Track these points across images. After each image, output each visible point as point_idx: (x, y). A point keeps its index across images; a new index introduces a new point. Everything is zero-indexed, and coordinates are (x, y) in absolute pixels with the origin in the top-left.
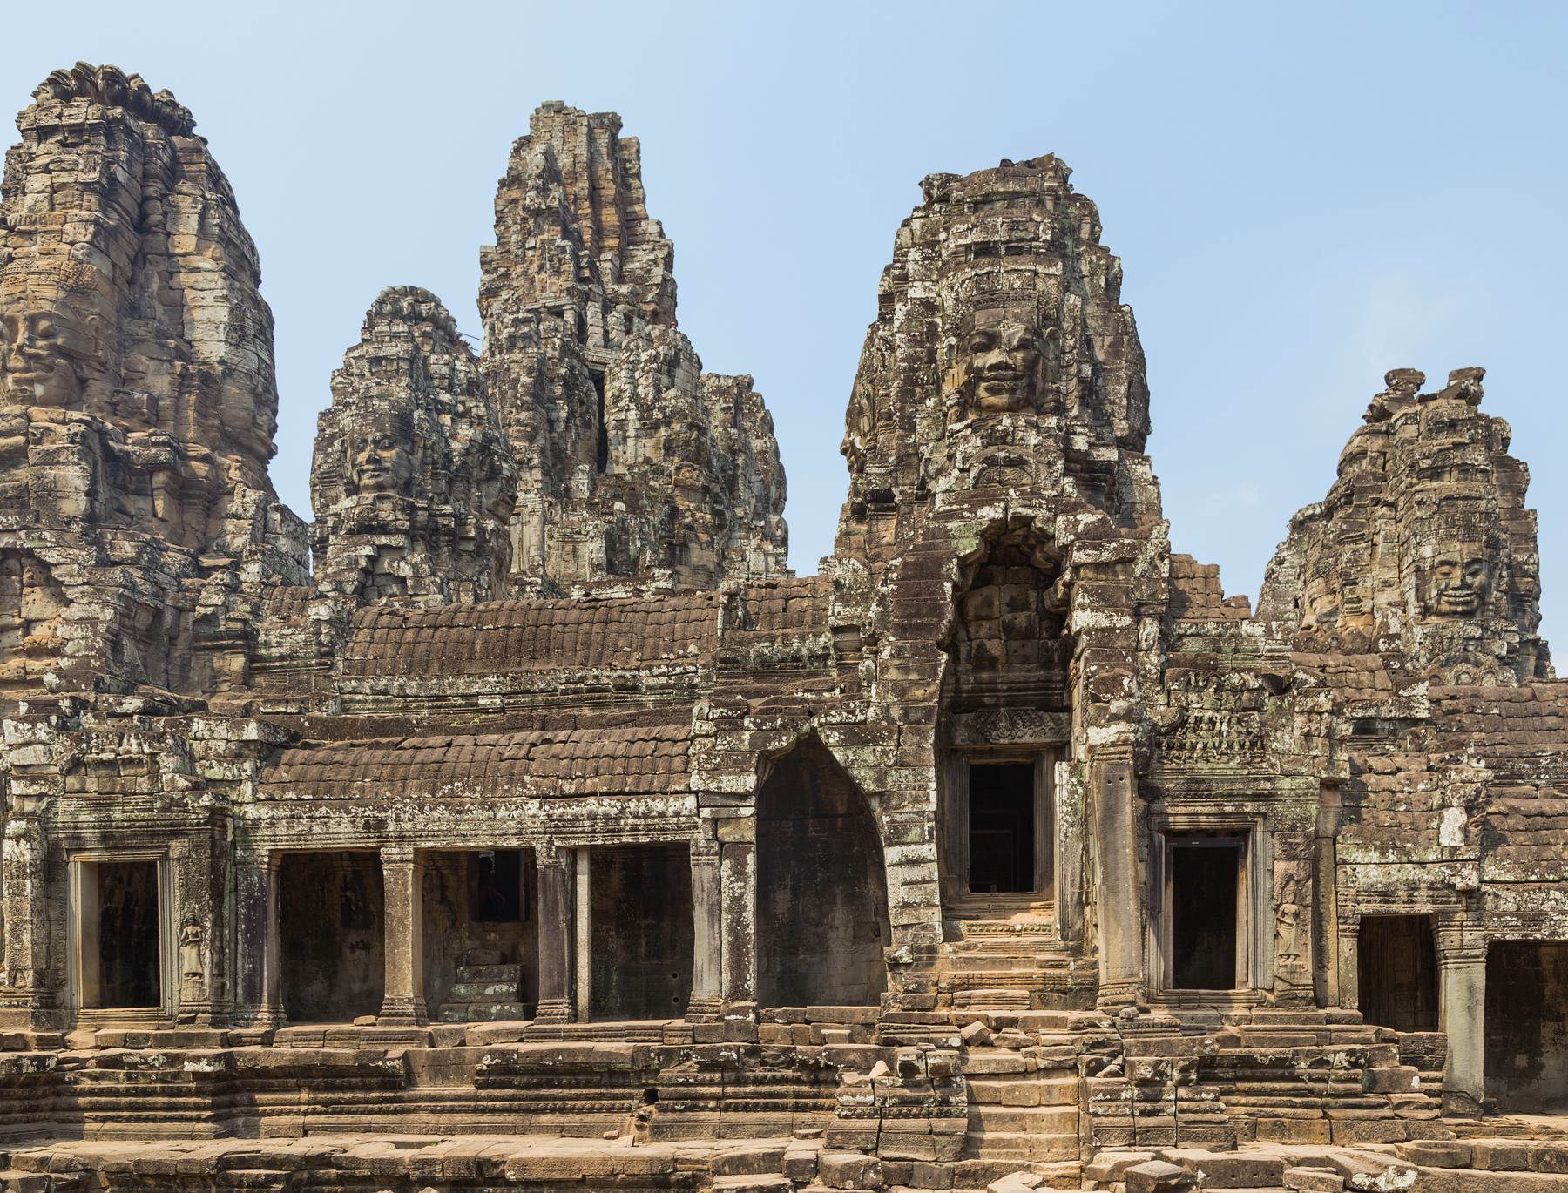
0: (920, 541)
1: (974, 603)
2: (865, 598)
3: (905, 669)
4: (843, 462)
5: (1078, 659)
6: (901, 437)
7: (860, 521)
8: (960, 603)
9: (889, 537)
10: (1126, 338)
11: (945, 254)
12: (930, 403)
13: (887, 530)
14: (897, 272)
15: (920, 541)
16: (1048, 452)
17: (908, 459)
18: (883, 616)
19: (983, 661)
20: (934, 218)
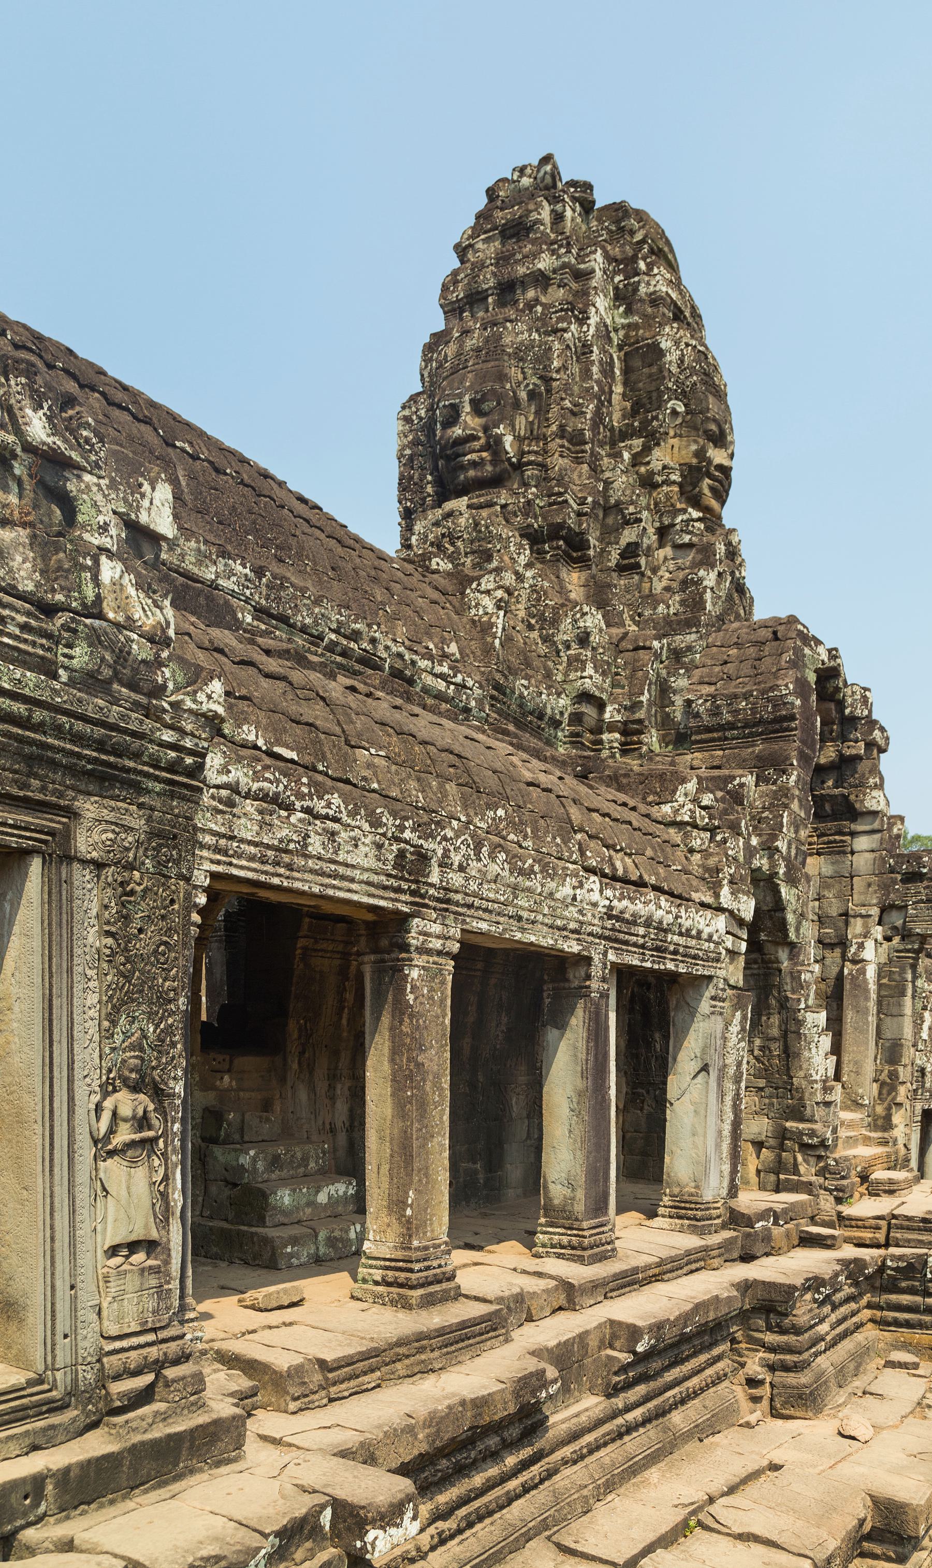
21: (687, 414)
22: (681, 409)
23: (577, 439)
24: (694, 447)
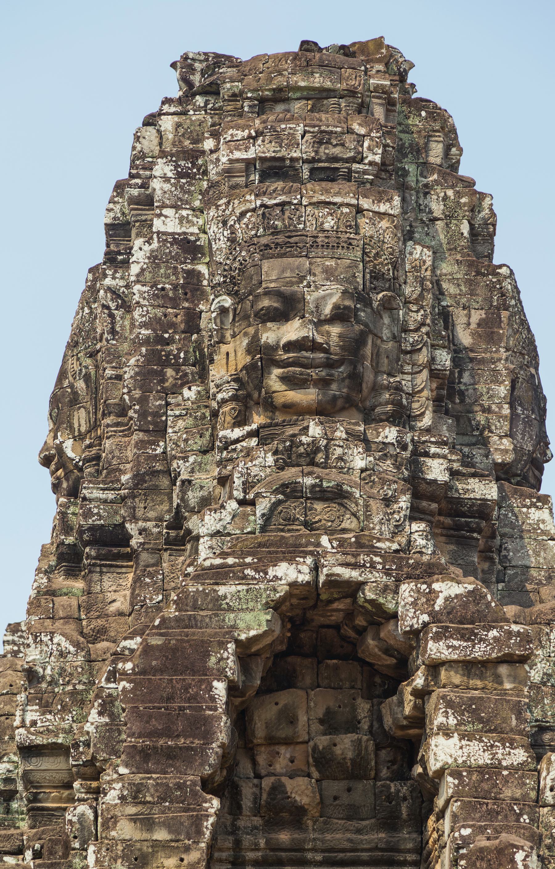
0: (172, 612)
1: (264, 716)
2: (79, 700)
3: (146, 823)
4: (45, 477)
5: (441, 816)
6: (141, 445)
7: (71, 573)
8: (241, 718)
9: (120, 601)
10: (505, 314)
11: (213, 171)
12: (190, 394)
13: (117, 590)
14: (135, 192)
15: (172, 612)
16: (383, 482)
17: (153, 479)
18: (110, 731)
19: (280, 811)
20: (195, 117)
22: (227, 302)
24: (245, 342)
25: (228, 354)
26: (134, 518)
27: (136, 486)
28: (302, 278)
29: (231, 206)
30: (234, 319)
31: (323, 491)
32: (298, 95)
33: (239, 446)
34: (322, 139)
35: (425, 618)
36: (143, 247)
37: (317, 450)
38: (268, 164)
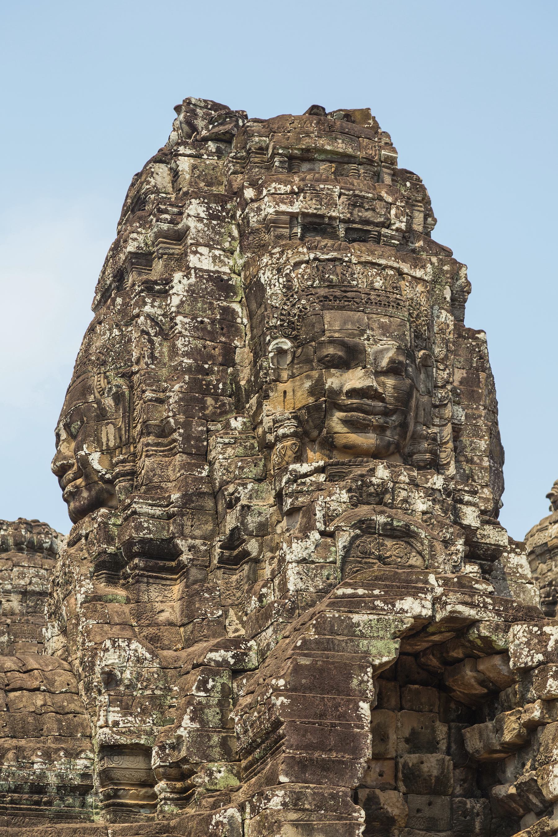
21: (298, 347)
22: (287, 344)
23: (164, 431)
24: (308, 384)
25: (285, 392)
26: (183, 536)
27: (184, 505)
28: (362, 332)
29: (285, 256)
30: (292, 362)
31: (393, 529)
32: (323, 157)
33: (307, 480)
34: (356, 202)
35: (540, 657)
36: (182, 281)
37: (386, 491)
38: (309, 219)
